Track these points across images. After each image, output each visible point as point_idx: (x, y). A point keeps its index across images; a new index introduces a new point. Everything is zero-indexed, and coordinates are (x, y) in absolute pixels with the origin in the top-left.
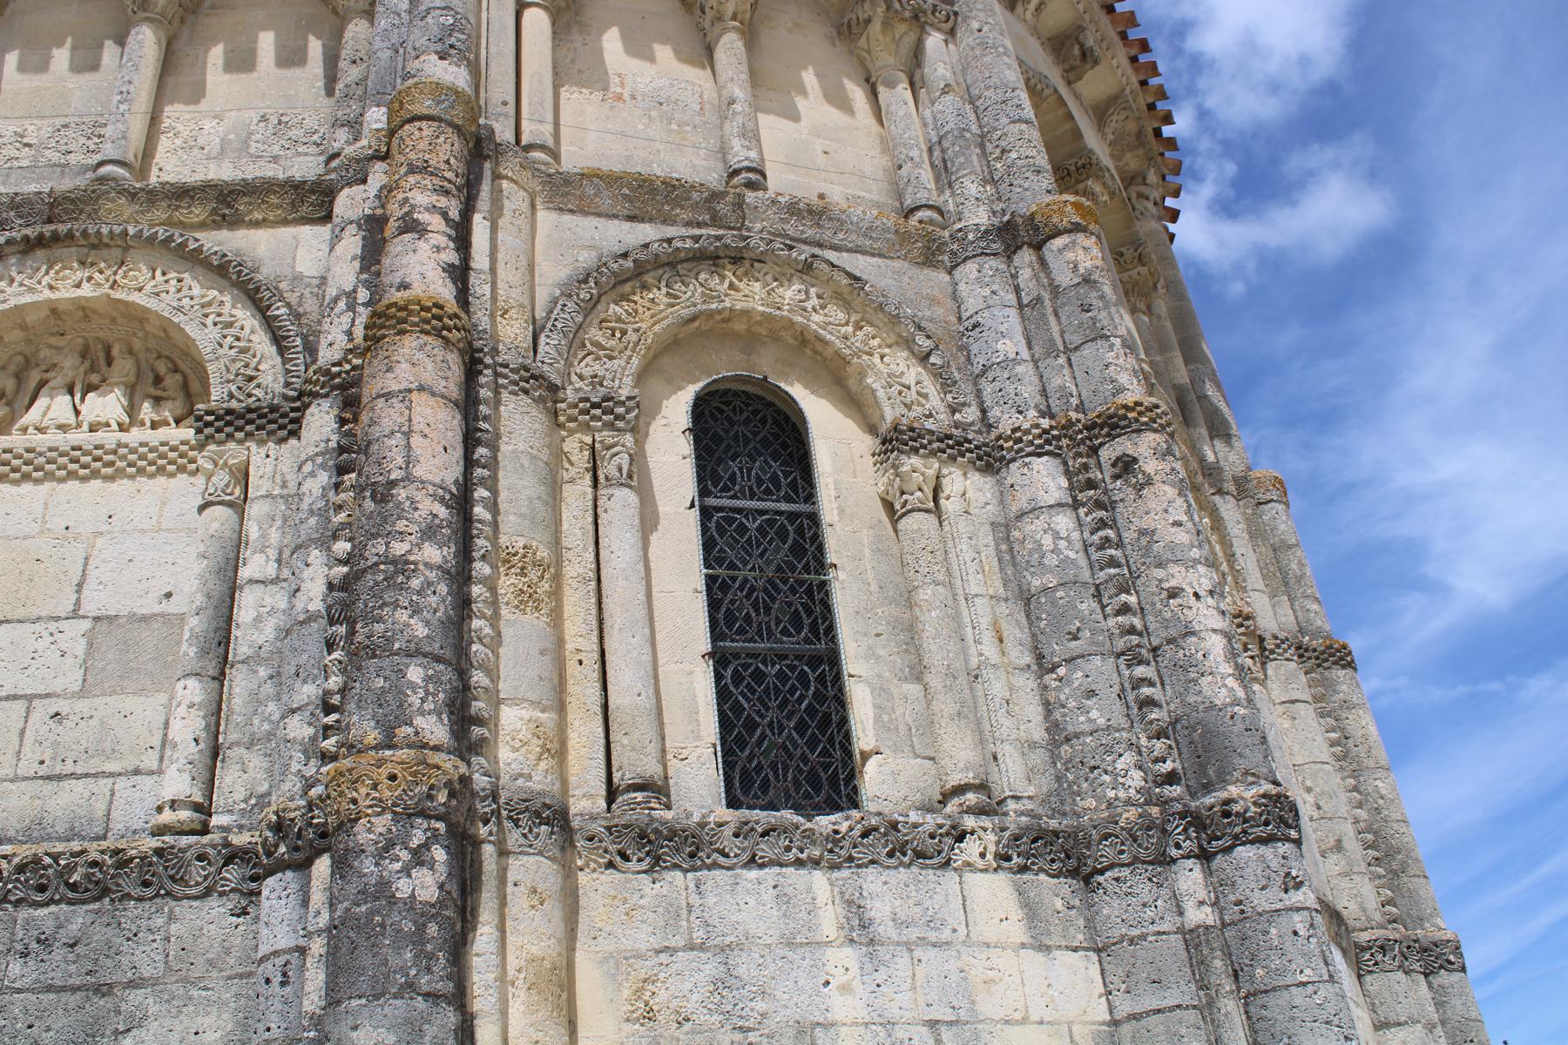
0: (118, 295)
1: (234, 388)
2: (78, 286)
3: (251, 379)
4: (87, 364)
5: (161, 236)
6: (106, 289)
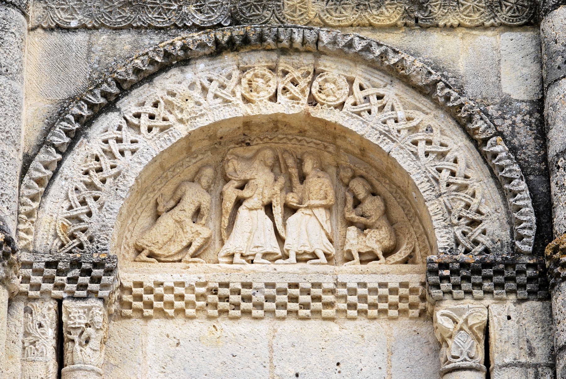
0: (318, 113)
1: (459, 234)
2: (274, 98)
3: (473, 223)
4: (282, 180)
5: (359, 46)
6: (303, 106)
